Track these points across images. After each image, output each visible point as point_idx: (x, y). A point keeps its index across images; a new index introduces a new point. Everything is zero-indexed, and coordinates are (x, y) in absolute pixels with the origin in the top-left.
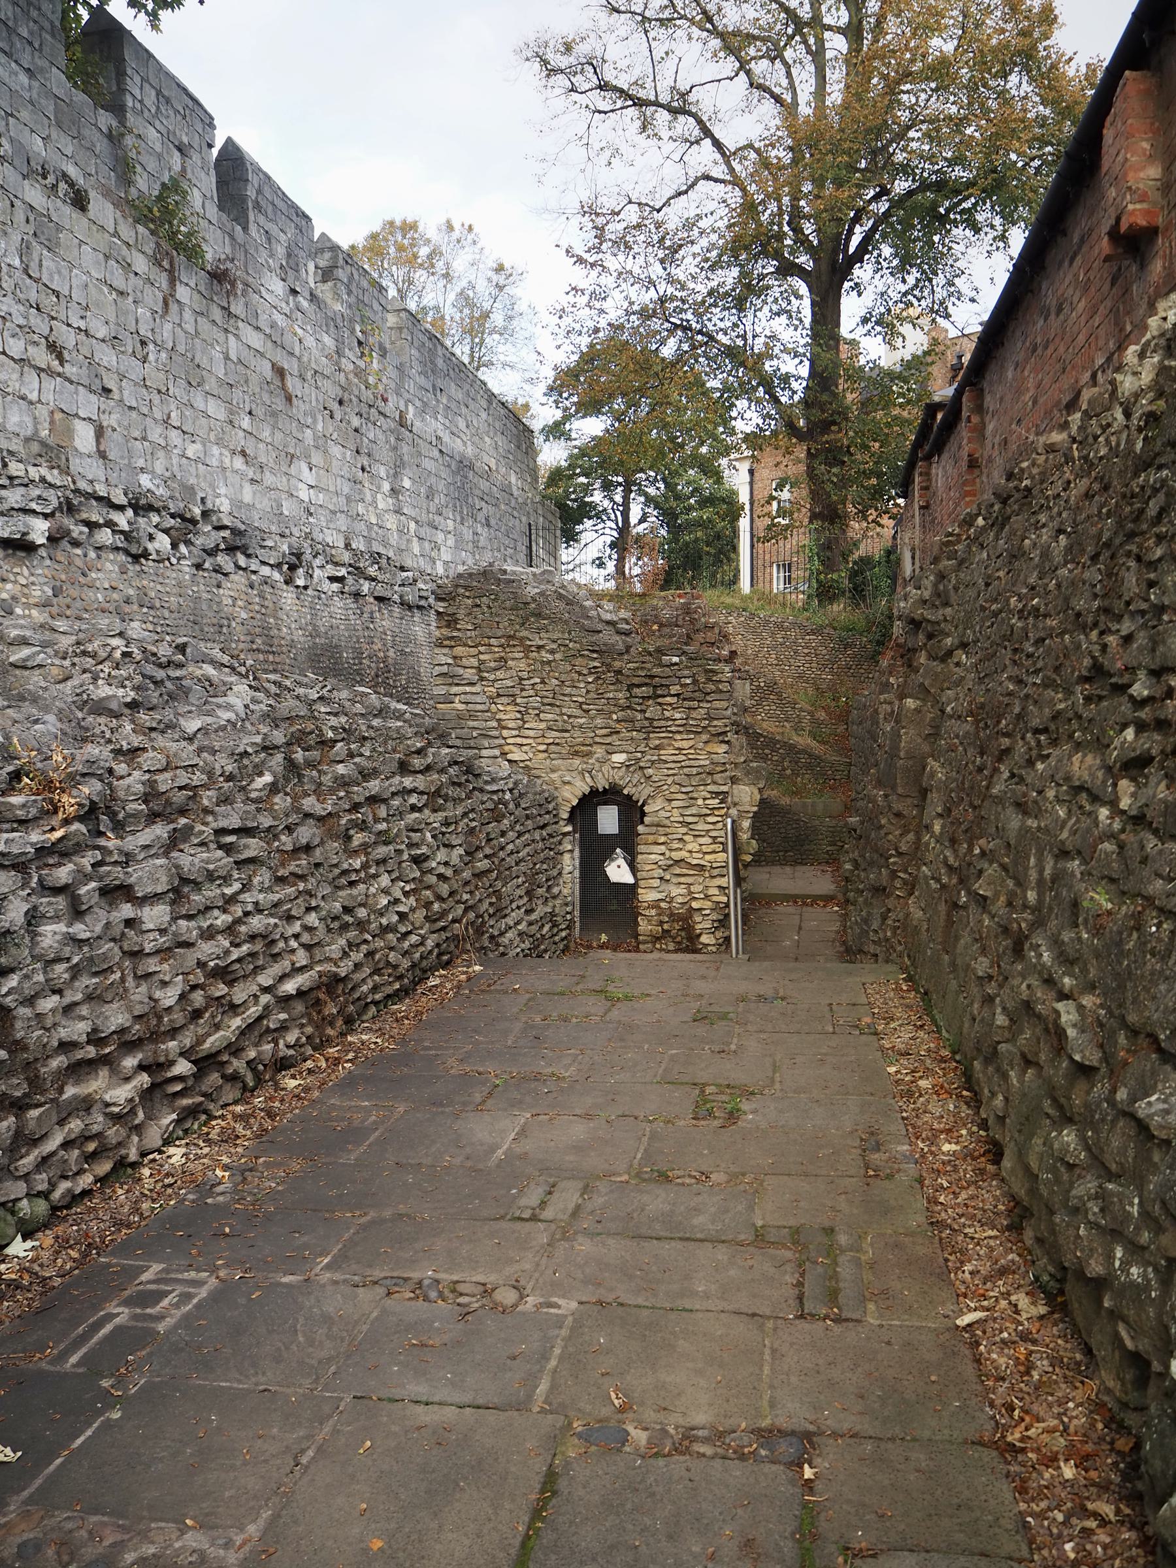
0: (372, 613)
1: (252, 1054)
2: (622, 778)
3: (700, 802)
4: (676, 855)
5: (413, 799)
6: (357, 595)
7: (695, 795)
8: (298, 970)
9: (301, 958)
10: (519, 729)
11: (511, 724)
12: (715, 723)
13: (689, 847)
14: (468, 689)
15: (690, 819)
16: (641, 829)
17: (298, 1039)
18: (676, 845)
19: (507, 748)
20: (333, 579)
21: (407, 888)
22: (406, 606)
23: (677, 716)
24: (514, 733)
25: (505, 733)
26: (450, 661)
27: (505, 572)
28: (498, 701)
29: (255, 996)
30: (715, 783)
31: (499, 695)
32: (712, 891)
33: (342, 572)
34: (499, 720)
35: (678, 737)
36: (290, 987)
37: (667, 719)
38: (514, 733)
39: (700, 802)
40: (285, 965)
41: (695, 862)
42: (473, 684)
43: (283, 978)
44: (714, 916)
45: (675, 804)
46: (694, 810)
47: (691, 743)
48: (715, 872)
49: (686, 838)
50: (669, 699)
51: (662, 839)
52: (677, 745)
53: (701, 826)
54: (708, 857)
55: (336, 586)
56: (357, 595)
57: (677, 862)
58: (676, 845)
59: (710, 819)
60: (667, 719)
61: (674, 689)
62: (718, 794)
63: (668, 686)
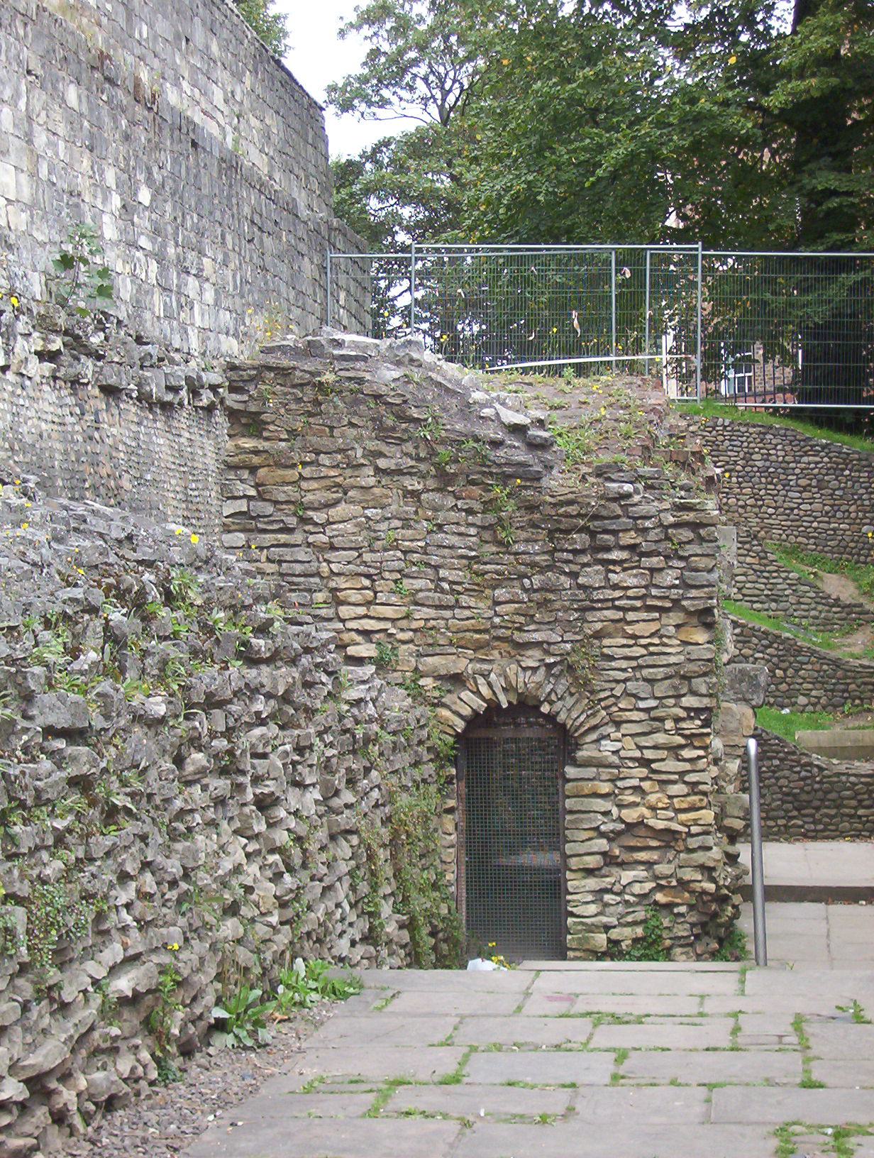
0: (96, 413)
1: (82, 1083)
2: (540, 685)
3: (669, 725)
4: (631, 815)
5: (260, 705)
6: (75, 383)
7: (659, 713)
8: (132, 960)
9: (136, 941)
10: (368, 603)
11: (355, 597)
12: (693, 593)
13: (652, 798)
14: (283, 538)
15: (649, 754)
16: (571, 771)
17: (133, 1070)
18: (629, 798)
19: (346, 637)
20: (43, 356)
21: (250, 849)
22: (145, 400)
23: (631, 581)
24: (361, 611)
25: (344, 611)
26: (253, 492)
27: (339, 344)
28: (331, 556)
29: (85, 992)
30: (694, 693)
31: (333, 548)
32: (688, 874)
33: (57, 344)
34: (334, 591)
35: (631, 616)
36: (124, 984)
37: (615, 587)
38: (361, 611)
39: (669, 725)
40: (114, 952)
41: (660, 825)
42: (289, 531)
43: (114, 970)
44: (693, 918)
45: (626, 728)
46: (660, 738)
47: (653, 627)
48: (693, 843)
49: (646, 785)
50: (615, 555)
51: (605, 788)
52: (629, 630)
53: (672, 765)
54: (683, 817)
55: (48, 367)
56: (75, 383)
57: (630, 827)
58: (629, 798)
59: (687, 753)
60: (615, 587)
61: (627, 539)
62: (698, 711)
63: (614, 533)
